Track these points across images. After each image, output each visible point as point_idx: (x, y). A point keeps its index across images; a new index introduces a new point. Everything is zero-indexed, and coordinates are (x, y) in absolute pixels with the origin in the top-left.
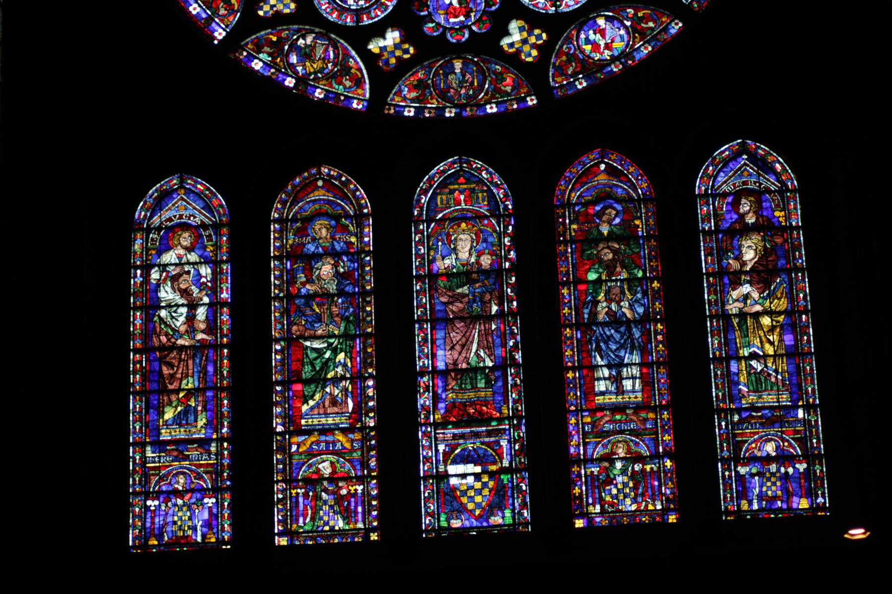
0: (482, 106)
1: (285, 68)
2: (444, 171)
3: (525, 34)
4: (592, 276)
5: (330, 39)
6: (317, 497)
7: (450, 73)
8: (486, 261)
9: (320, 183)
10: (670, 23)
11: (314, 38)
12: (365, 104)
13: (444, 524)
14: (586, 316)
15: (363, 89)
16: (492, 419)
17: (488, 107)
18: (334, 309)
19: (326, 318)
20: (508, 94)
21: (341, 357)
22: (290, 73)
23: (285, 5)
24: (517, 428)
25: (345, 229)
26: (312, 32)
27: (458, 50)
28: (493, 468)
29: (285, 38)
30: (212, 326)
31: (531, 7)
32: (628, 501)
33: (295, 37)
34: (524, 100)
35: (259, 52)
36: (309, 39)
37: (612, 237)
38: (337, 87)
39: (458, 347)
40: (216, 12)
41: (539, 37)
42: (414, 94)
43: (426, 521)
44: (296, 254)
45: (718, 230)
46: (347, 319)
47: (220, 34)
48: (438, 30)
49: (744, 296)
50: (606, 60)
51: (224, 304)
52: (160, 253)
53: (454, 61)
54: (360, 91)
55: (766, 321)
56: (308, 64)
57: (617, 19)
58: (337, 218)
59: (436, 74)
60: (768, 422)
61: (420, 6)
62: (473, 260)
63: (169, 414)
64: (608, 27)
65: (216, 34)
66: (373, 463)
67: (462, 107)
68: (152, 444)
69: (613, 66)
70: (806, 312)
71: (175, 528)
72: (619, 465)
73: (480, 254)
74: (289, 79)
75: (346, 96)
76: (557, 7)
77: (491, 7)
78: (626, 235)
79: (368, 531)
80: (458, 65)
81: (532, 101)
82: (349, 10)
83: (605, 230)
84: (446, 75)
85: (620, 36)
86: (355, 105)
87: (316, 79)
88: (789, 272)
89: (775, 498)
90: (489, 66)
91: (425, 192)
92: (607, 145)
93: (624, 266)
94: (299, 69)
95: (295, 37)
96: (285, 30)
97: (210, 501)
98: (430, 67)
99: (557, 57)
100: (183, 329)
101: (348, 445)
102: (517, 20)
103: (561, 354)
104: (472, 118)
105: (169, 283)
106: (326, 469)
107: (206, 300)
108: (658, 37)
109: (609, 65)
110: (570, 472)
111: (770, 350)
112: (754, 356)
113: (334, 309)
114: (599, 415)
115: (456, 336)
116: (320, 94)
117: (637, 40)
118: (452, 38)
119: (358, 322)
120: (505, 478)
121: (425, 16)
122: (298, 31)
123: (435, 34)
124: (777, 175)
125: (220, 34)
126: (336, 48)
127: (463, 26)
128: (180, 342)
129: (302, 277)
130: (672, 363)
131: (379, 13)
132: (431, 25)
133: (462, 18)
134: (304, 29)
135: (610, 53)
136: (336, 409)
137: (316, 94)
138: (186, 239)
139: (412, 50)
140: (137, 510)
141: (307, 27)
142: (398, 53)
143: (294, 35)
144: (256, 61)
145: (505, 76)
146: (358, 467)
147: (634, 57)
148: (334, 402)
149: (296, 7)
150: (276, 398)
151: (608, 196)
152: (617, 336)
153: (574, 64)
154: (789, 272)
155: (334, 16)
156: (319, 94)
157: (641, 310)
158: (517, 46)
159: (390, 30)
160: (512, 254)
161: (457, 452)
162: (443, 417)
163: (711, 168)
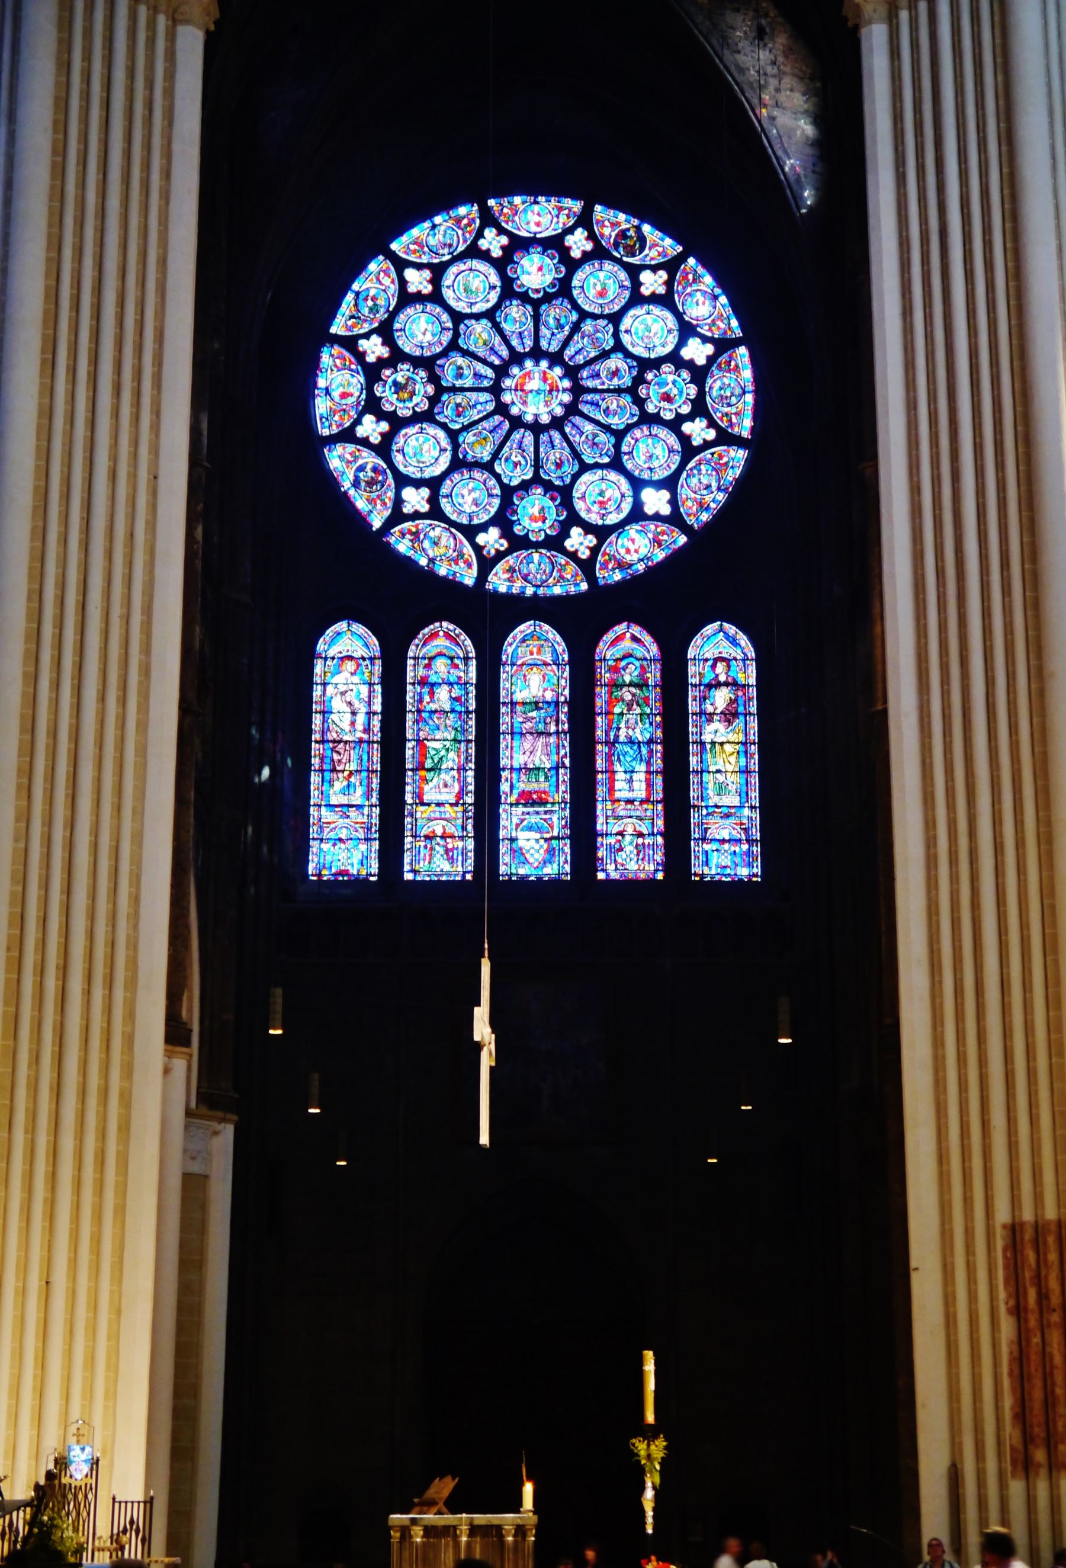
2: (521, 632)
4: (617, 710)
6: (431, 849)
8: (549, 696)
9: (441, 633)
13: (514, 871)
14: (612, 737)
16: (547, 802)
18: (448, 721)
19: (442, 727)
20: (568, 580)
21: (452, 755)
24: (564, 809)
25: (456, 666)
28: (547, 836)
30: (367, 730)
32: (633, 863)
34: (577, 585)
36: (438, 530)
37: (631, 684)
39: (528, 753)
42: (507, 576)
43: (503, 869)
44: (423, 682)
45: (700, 685)
46: (456, 729)
47: (377, 523)
49: (715, 731)
51: (375, 713)
52: (333, 676)
55: (728, 748)
58: (451, 658)
60: (727, 816)
62: (540, 694)
63: (338, 785)
66: (470, 828)
68: (326, 806)
70: (754, 743)
71: (340, 864)
72: (628, 838)
73: (545, 690)
78: (642, 685)
79: (465, 873)
80: (536, 556)
81: (584, 586)
83: (627, 679)
84: (528, 564)
88: (745, 715)
89: (725, 867)
91: (510, 645)
92: (632, 619)
93: (638, 705)
97: (363, 847)
98: (518, 557)
100: (347, 728)
101: (454, 815)
103: (594, 761)
105: (339, 695)
106: (439, 832)
107: (364, 710)
110: (596, 841)
111: (730, 768)
112: (718, 771)
113: (448, 721)
114: (616, 805)
115: (527, 745)
118: (532, 537)
119: (464, 731)
120: (554, 843)
124: (742, 649)
126: (455, 539)
128: (345, 738)
129: (427, 698)
130: (665, 773)
132: (519, 527)
136: (446, 790)
138: (350, 666)
140: (315, 850)
142: (497, 546)
146: (460, 830)
148: (446, 786)
150: (408, 780)
151: (630, 655)
152: (631, 752)
154: (745, 715)
156: (442, 571)
157: (648, 736)
160: (567, 692)
161: (525, 823)
162: (517, 800)
163: (699, 641)
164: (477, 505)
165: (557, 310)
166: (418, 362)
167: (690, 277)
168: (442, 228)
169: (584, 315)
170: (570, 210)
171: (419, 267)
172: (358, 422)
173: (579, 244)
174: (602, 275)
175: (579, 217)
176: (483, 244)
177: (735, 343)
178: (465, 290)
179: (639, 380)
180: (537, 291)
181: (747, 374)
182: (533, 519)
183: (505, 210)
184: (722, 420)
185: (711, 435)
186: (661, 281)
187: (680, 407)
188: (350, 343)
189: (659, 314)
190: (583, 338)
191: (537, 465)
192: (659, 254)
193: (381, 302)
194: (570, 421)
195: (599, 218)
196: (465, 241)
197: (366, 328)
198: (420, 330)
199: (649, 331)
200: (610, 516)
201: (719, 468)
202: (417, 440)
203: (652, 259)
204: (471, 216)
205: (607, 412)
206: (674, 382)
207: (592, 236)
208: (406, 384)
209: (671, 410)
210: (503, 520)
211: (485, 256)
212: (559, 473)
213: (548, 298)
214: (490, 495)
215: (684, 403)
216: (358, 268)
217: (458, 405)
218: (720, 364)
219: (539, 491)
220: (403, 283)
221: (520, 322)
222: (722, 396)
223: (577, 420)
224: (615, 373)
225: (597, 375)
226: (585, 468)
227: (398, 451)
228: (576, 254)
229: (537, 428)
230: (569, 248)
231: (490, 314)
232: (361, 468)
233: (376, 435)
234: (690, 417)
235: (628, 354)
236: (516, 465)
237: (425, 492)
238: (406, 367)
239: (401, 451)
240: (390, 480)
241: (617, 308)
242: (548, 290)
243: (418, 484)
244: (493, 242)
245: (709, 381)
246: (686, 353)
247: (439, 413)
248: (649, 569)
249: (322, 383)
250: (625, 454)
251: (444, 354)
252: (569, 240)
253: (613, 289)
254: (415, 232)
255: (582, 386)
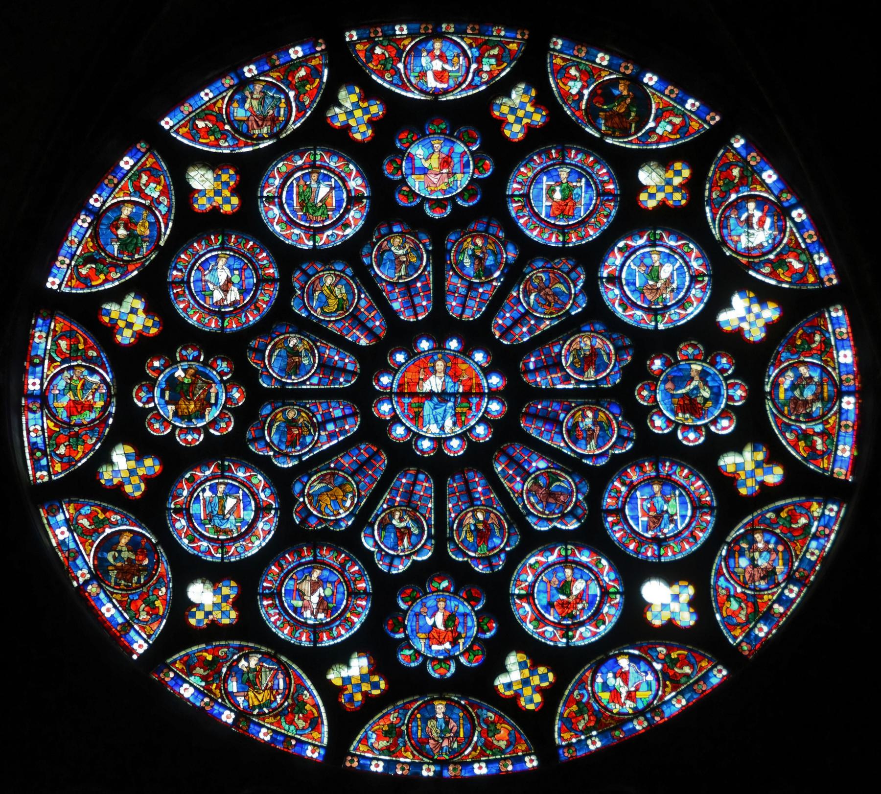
0: (467, 765)
1: (222, 697)
3: (526, 672)
5: (279, 662)
7: (430, 719)
10: (711, 670)
11: (260, 660)
12: (322, 752)
15: (320, 733)
17: (476, 766)
20: (502, 751)
22: (229, 705)
23: (223, 612)
26: (257, 651)
27: (441, 688)
29: (222, 658)
31: (536, 636)
33: (235, 657)
34: (520, 760)
35: (190, 673)
36: (254, 661)
38: (287, 727)
40: (135, 616)
41: (543, 678)
47: (140, 646)
48: (417, 659)
50: (628, 714)
53: (436, 703)
54: (316, 735)
56: (251, 694)
57: (645, 660)
59: (412, 718)
61: (394, 625)
64: (632, 670)
65: (135, 646)
67: (444, 764)
69: (635, 723)
74: (227, 712)
75: (298, 740)
76: (569, 638)
77: (484, 632)
80: (440, 708)
81: (531, 763)
82: (305, 624)
84: (425, 721)
85: (647, 682)
86: (309, 753)
87: (261, 715)
90: (479, 711)
94: (240, 699)
95: (235, 657)
96: (222, 646)
98: (405, 708)
99: (567, 705)
102: (518, 652)
104: (457, 781)
108: (695, 687)
109: (631, 720)
116: (265, 735)
117: (668, 690)
121: (401, 640)
122: (240, 649)
123: (413, 665)
125: (140, 646)
126: (287, 675)
127: (449, 657)
131: (343, 632)
132: (407, 652)
133: (448, 646)
134: (247, 646)
135: (633, 705)
137: (261, 736)
139: (383, 685)
141: (251, 644)
142: (366, 687)
143: (234, 654)
144: (186, 686)
145: (499, 726)
147: (663, 712)
149: (238, 617)
153: (586, 716)
155: (286, 631)
156: (264, 735)
158: (515, 688)
159: (356, 655)
164: (328, 611)
165: (479, 242)
166: (215, 344)
167: (736, 172)
168: (258, 87)
169: (530, 251)
170: (502, 45)
171: (213, 162)
172: (103, 457)
173: (520, 113)
174: (564, 173)
175: (520, 60)
176: (338, 116)
177: (824, 298)
178: (302, 205)
179: (637, 373)
180: (439, 204)
181: (846, 356)
182: (432, 635)
183: (378, 51)
184: (796, 447)
185: (775, 476)
186: (677, 181)
187: (714, 422)
188: (85, 311)
189: (672, 243)
190: (527, 294)
191: (441, 536)
192: (676, 130)
193: (143, 230)
194: (504, 452)
195: (558, 61)
196: (301, 109)
197: (115, 279)
198: (219, 282)
199: (655, 277)
200: (582, 629)
201: (790, 540)
202: (213, 489)
203: (661, 139)
204: (314, 63)
205: (574, 434)
206: (703, 375)
207: (544, 99)
208: (193, 384)
209: (697, 429)
210: (377, 641)
211: (339, 140)
212: (483, 550)
213: (460, 220)
214: (353, 594)
215: (724, 414)
216: (100, 170)
217: (291, 424)
218: (794, 339)
219: (445, 584)
220: (184, 193)
221: (409, 264)
222: (795, 400)
223: (517, 451)
224: (592, 359)
225: (555, 365)
226: (533, 541)
227: (177, 511)
228: (515, 131)
229: (440, 466)
230: (502, 122)
231: (349, 253)
232: (110, 543)
233: (135, 480)
234: (734, 443)
235: (614, 326)
236: (401, 534)
237: (229, 589)
238: (191, 353)
239: (184, 511)
240: (164, 567)
241: (593, 234)
242: (460, 202)
243: (215, 574)
244: (353, 112)
245: (774, 373)
246: (728, 319)
247: (254, 440)
248: (652, 729)
249: (33, 384)
250: (610, 512)
251: (264, 328)
252: (502, 108)
253: (585, 198)
254: (206, 95)
255: (527, 385)
